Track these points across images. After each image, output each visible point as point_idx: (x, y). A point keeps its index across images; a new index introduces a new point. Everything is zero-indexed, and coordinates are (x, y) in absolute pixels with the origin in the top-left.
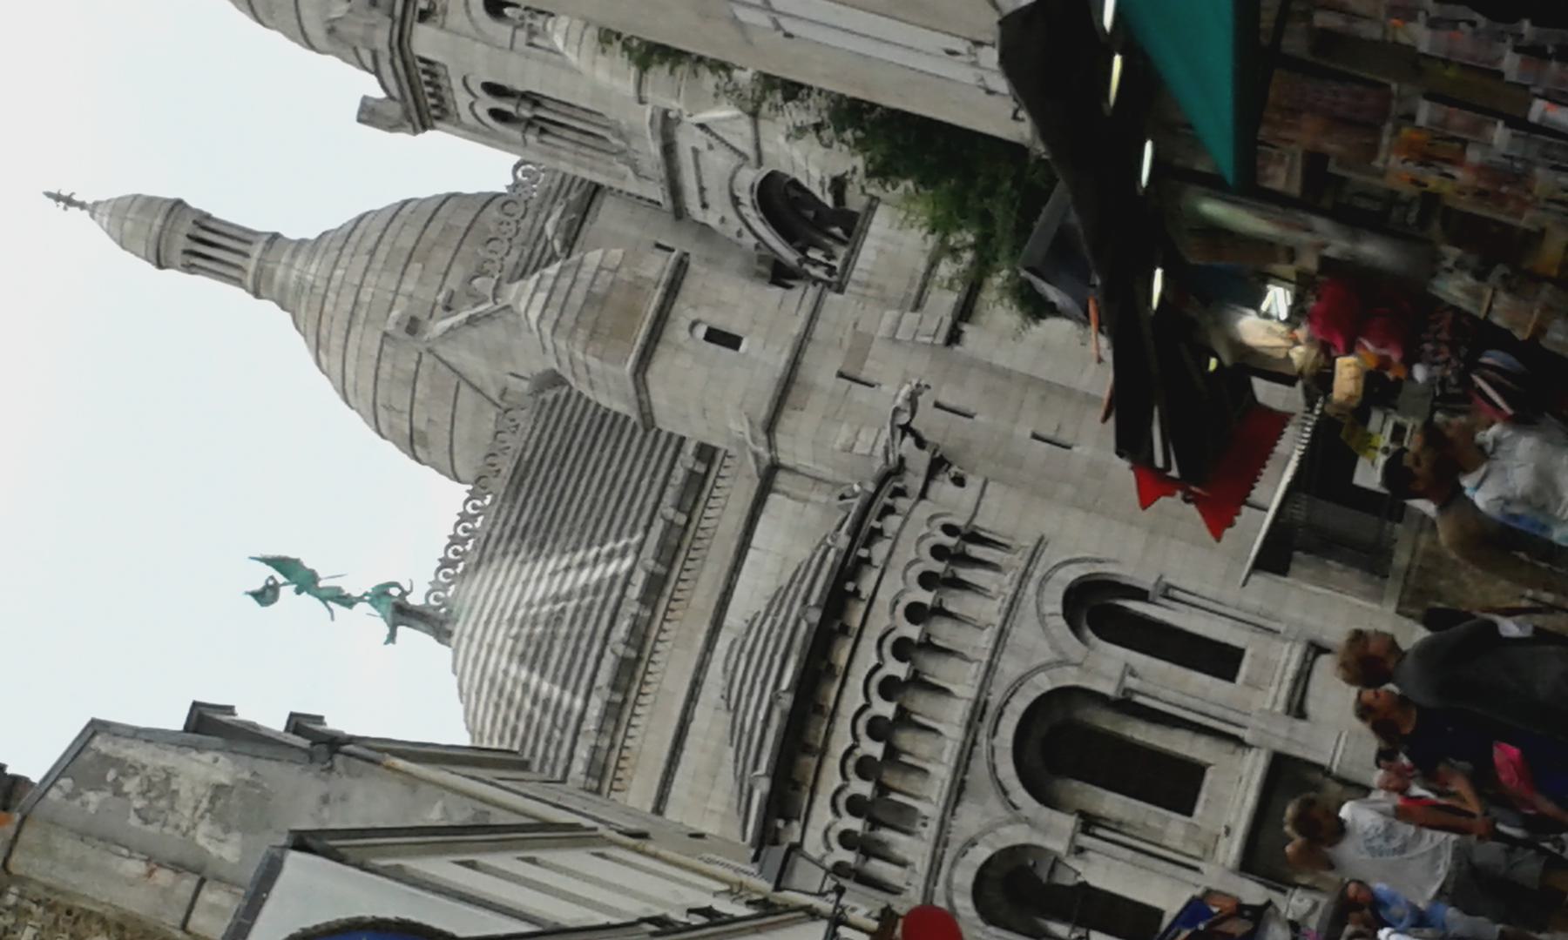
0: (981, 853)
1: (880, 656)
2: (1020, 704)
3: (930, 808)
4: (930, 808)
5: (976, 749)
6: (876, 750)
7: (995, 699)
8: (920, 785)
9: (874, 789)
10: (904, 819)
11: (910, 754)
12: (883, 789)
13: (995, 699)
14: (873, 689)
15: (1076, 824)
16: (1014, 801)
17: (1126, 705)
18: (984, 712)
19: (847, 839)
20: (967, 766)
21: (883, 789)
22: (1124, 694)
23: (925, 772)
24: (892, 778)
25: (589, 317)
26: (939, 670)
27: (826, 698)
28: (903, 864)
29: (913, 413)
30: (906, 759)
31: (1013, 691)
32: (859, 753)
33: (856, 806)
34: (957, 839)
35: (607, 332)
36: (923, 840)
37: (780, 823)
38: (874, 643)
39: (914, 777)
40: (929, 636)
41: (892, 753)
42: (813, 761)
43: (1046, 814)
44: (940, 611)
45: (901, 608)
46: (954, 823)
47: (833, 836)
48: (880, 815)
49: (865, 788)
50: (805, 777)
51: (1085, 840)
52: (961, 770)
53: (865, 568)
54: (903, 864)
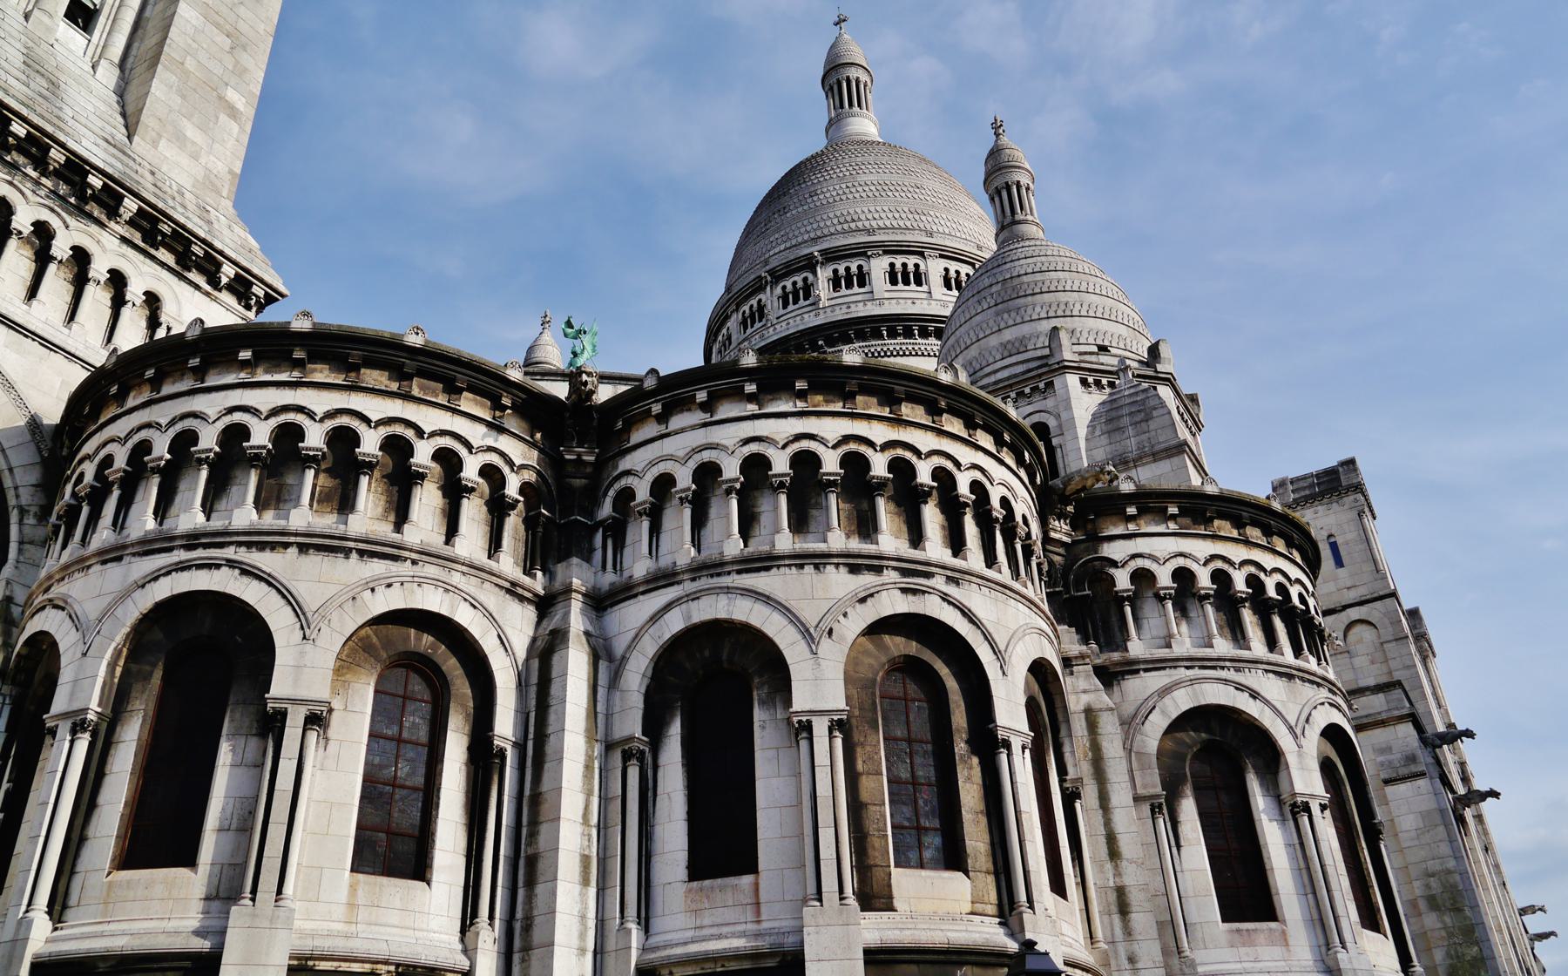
47: (1181, 562)
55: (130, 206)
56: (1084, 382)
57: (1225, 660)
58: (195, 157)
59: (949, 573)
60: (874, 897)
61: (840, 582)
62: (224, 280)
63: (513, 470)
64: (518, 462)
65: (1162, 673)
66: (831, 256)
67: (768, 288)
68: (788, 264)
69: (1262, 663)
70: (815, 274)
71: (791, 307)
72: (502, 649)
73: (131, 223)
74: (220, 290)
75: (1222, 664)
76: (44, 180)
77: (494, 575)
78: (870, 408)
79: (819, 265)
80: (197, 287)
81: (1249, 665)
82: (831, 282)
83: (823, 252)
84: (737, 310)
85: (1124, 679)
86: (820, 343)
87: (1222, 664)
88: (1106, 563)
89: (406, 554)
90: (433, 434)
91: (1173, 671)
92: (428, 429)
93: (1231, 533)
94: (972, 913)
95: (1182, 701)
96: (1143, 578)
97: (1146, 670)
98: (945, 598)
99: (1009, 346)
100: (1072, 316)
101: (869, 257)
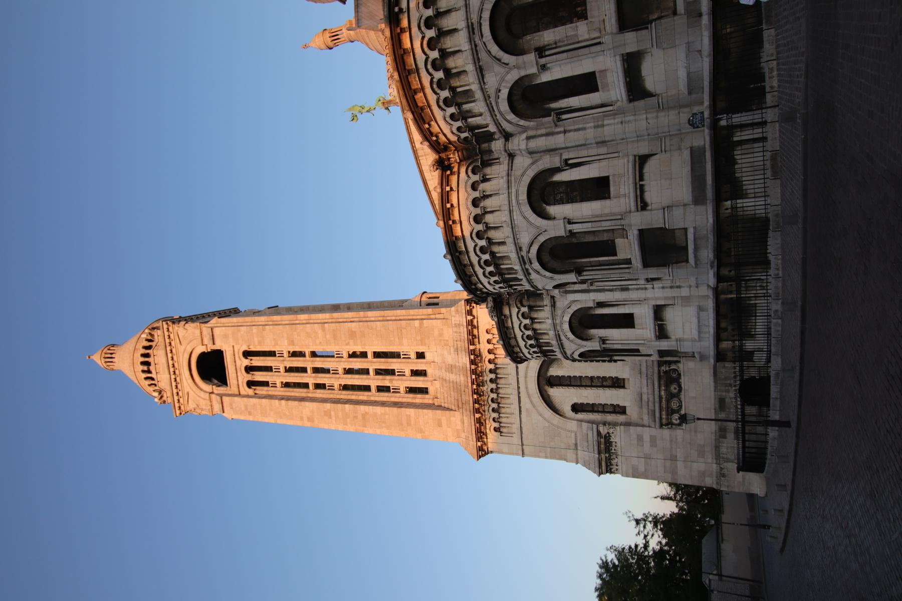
0: (505, 93)
2: (486, 15)
3: (475, 87)
5: (478, 48)
6: (440, 75)
7: (474, 18)
8: (467, 79)
9: (449, 91)
11: (456, 68)
12: (453, 89)
13: (474, 18)
15: (535, 56)
16: (505, 62)
18: (473, 29)
20: (478, 59)
21: (453, 89)
23: (465, 71)
24: (455, 83)
26: (447, 23)
27: (412, 66)
28: (481, 115)
30: (454, 71)
31: (481, 10)
32: (435, 80)
33: (447, 102)
34: (491, 91)
36: (480, 101)
37: (427, 126)
38: (417, 28)
40: (437, 9)
41: (448, 72)
43: (521, 58)
46: (486, 87)
47: (448, 119)
48: (459, 101)
49: (445, 94)
50: (423, 103)
51: (543, 61)
52: (477, 61)
54: (481, 115)
55: (472, 347)
57: (487, 104)
58: (442, 329)
59: (519, 251)
60: (628, 262)
61: (534, 276)
62: (472, 317)
63: (520, 310)
64: (517, 310)
69: (481, 86)
72: (571, 307)
73: (474, 344)
74: (474, 316)
75: (489, 104)
76: (479, 366)
77: (552, 313)
78: (471, 272)
80: (477, 321)
87: (489, 104)
89: (557, 333)
90: (522, 332)
92: (521, 334)
93: (421, 97)
94: (627, 238)
95: (511, 117)
96: (459, 129)
97: (502, 127)
98: (529, 252)
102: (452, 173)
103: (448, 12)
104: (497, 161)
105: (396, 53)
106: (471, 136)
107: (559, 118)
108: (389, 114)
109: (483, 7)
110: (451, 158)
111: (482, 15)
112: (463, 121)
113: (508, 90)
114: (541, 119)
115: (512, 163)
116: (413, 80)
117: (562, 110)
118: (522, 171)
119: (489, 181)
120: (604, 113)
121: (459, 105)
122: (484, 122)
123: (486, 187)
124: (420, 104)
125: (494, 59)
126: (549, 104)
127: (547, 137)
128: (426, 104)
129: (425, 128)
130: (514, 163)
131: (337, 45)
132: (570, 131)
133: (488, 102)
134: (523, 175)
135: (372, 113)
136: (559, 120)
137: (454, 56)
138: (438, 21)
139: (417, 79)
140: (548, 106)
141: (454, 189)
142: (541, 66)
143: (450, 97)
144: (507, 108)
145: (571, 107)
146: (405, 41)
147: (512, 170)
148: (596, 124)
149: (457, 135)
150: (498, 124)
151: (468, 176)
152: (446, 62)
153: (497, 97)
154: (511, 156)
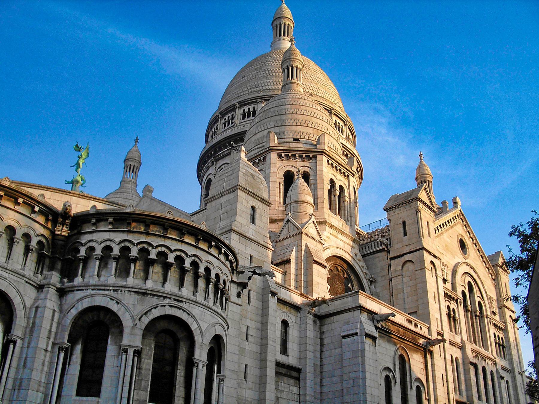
0: (114, 307)
1: (191, 256)
2: (184, 316)
4: (130, 281)
5: (162, 298)
8: (139, 277)
10: (124, 272)
12: (135, 260)
14: (177, 253)
17: (190, 364)
19: (108, 249)
20: (154, 295)
21: (135, 260)
22: (196, 363)
25: (249, 174)
27: (170, 234)
29: (259, 275)
32: (150, 248)
33: (125, 250)
34: (119, 296)
35: (247, 179)
37: (111, 220)
39: (142, 274)
41: (152, 262)
42: (142, 229)
43: (140, 333)
44: (208, 282)
45: (208, 265)
47: (108, 243)
48: (121, 262)
49: (134, 252)
51: (131, 352)
52: (153, 293)
53: (217, 252)
56: (280, 156)
65: (82, 292)
66: (242, 104)
67: (219, 120)
68: (226, 109)
69: (129, 288)
70: (236, 112)
71: (226, 128)
79: (238, 108)
81: (121, 289)
82: (242, 115)
83: (239, 103)
84: (211, 130)
85: (68, 294)
86: (231, 143)
87: (108, 288)
88: (79, 244)
91: (86, 291)
93: (140, 229)
95: (86, 304)
96: (92, 249)
97: (77, 290)
99: (257, 141)
100: (285, 125)
101: (258, 103)
102: (47, 220)
103: (196, 285)
104: (40, 271)
105: (186, 227)
106: (78, 257)
107: (62, 350)
108: (66, 181)
109: (190, 316)
110: (63, 228)
111: (185, 313)
112: (100, 256)
113: (115, 311)
114: (69, 332)
115: (33, 285)
116: (158, 230)
117: (69, 355)
118: (22, 292)
119: (24, 254)
120: (50, 395)
121: (116, 259)
122: (87, 275)
123: (19, 248)
124: (134, 224)
125: (149, 309)
126: (81, 344)
127: (48, 331)
128: (131, 230)
129: (109, 218)
130: (32, 287)
131: (124, 168)
132: (45, 356)
133: (111, 288)
134: (18, 291)
135: (74, 166)
136: (61, 349)
137: (162, 274)
138: (192, 274)
139: (157, 233)
140: (81, 343)
141: (32, 215)
142: (127, 349)
143: (130, 255)
144: (97, 304)
145: (69, 364)
146: (190, 239)
147: (26, 282)
148: (42, 384)
149: (86, 244)
150: (80, 288)
151: (38, 235)
152: (160, 265)
153: (112, 298)
154: (40, 288)
